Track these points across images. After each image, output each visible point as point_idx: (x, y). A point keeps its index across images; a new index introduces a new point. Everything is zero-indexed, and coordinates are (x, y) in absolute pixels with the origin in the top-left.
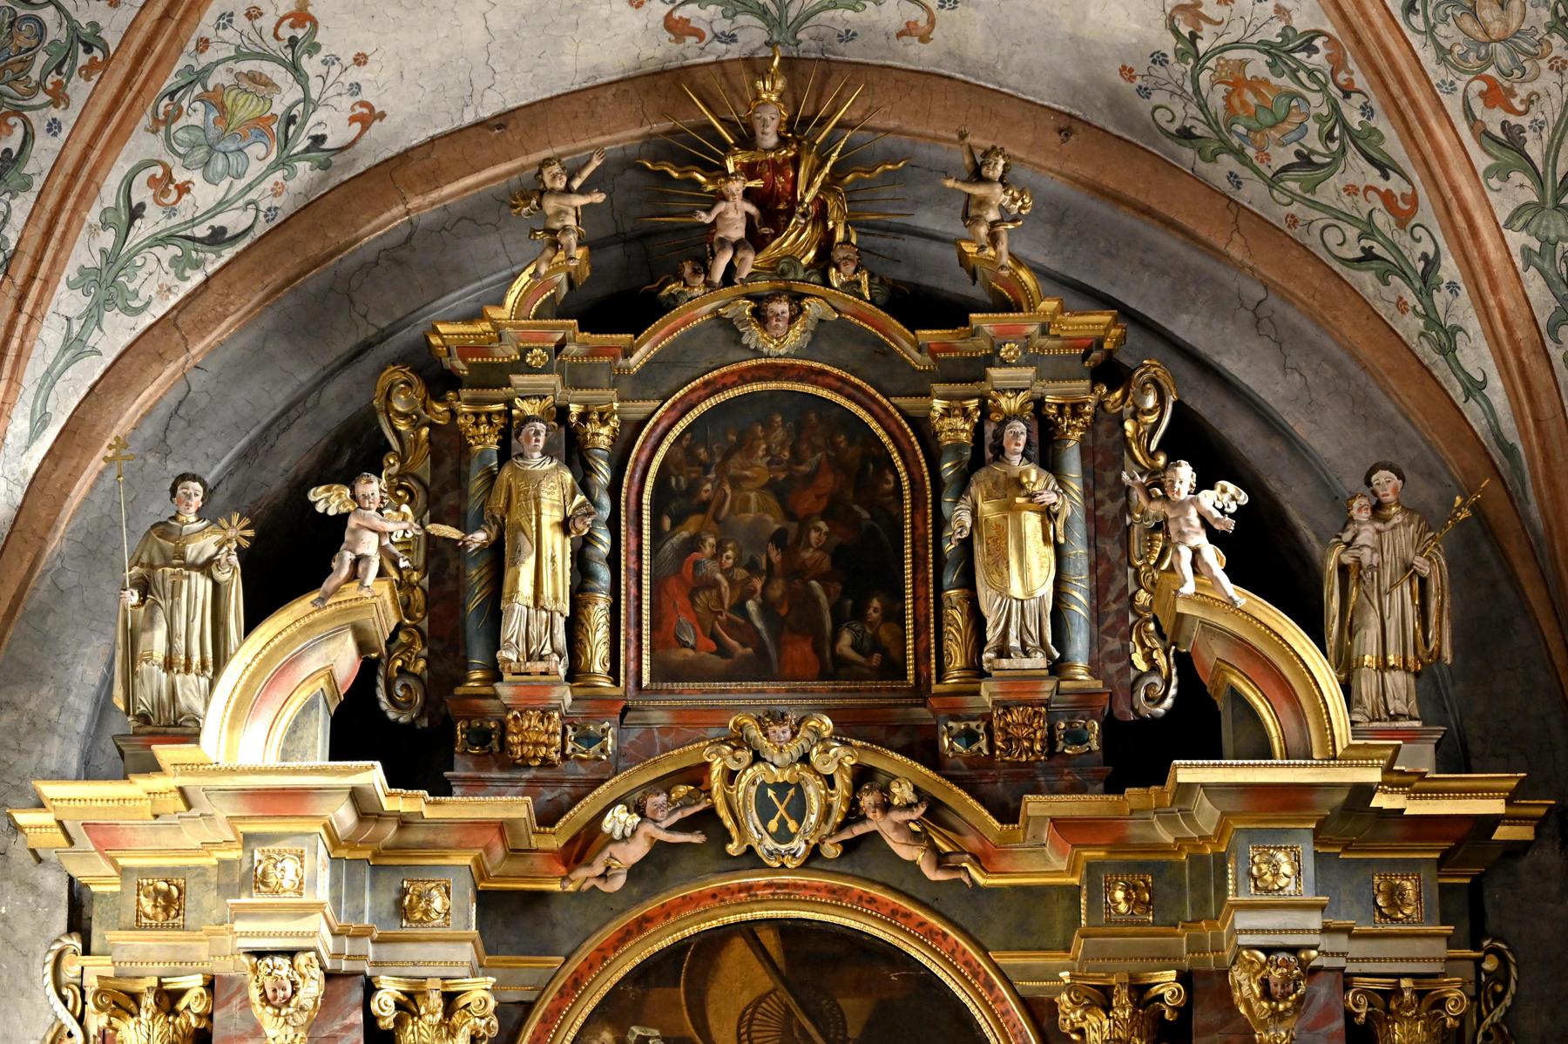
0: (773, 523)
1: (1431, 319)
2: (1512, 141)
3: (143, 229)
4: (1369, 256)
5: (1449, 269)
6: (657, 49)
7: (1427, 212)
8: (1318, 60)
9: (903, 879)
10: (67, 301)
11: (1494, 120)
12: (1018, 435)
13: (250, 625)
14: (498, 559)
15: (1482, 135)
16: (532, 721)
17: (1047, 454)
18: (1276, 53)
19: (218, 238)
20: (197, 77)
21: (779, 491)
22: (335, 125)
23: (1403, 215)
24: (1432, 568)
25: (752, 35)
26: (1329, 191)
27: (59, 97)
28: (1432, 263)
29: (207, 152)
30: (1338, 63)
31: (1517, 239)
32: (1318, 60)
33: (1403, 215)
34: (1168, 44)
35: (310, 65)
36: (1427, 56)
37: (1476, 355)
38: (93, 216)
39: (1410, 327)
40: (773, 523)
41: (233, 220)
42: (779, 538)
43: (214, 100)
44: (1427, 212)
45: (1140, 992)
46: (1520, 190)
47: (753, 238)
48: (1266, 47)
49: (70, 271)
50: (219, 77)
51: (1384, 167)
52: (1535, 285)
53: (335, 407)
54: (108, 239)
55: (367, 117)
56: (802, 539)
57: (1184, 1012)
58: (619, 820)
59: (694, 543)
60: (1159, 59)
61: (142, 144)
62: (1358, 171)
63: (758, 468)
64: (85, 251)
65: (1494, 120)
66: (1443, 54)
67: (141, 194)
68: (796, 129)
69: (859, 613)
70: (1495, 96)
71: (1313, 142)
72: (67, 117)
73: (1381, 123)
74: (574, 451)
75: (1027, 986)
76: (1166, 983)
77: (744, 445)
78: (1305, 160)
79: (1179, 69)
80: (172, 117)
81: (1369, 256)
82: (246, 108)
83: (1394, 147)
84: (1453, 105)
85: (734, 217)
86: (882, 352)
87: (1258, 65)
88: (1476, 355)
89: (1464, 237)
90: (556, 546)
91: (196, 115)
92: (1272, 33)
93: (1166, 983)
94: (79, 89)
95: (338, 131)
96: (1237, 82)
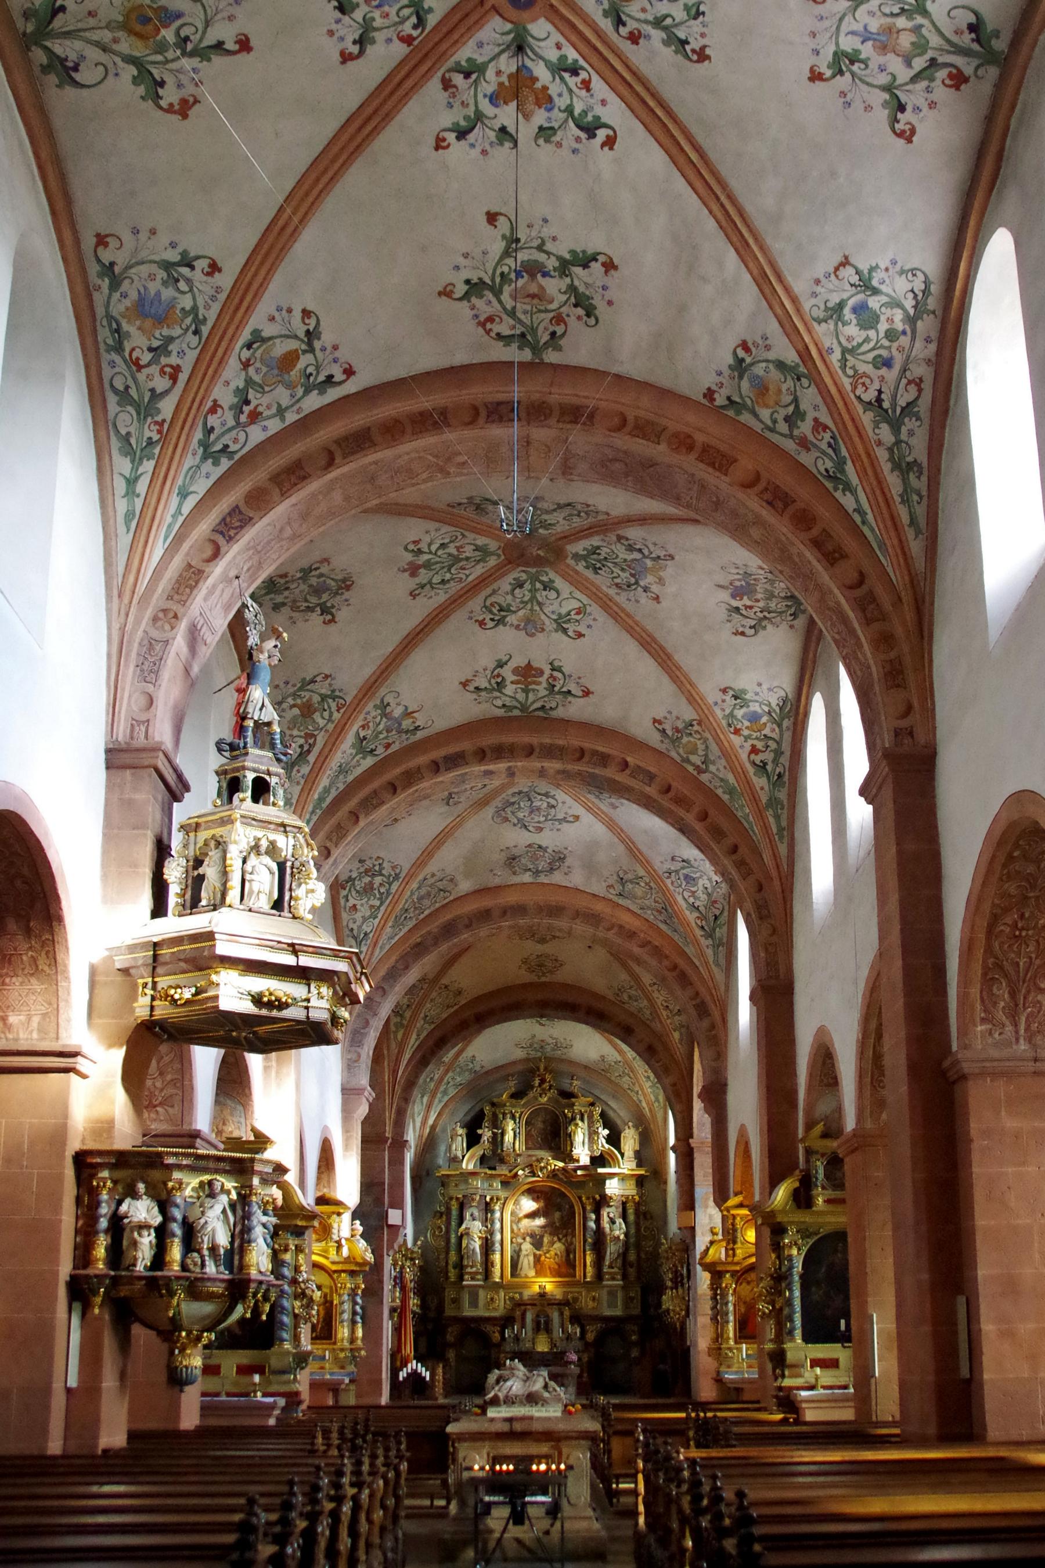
9: (560, 1180)
10: (439, 1095)
13: (468, 1149)
14: (503, 1134)
17: (582, 1120)
22: (478, 1068)
24: (637, 1137)
25: (539, 1054)
29: (460, 1074)
37: (644, 1104)
45: (594, 1199)
46: (649, 1084)
53: (477, 1109)
58: (520, 1172)
61: (450, 1074)
64: (442, 1088)
68: (546, 1069)
74: (513, 1117)
76: (597, 1197)
85: (537, 1082)
89: (642, 1090)
90: (511, 1133)
93: (597, 1197)
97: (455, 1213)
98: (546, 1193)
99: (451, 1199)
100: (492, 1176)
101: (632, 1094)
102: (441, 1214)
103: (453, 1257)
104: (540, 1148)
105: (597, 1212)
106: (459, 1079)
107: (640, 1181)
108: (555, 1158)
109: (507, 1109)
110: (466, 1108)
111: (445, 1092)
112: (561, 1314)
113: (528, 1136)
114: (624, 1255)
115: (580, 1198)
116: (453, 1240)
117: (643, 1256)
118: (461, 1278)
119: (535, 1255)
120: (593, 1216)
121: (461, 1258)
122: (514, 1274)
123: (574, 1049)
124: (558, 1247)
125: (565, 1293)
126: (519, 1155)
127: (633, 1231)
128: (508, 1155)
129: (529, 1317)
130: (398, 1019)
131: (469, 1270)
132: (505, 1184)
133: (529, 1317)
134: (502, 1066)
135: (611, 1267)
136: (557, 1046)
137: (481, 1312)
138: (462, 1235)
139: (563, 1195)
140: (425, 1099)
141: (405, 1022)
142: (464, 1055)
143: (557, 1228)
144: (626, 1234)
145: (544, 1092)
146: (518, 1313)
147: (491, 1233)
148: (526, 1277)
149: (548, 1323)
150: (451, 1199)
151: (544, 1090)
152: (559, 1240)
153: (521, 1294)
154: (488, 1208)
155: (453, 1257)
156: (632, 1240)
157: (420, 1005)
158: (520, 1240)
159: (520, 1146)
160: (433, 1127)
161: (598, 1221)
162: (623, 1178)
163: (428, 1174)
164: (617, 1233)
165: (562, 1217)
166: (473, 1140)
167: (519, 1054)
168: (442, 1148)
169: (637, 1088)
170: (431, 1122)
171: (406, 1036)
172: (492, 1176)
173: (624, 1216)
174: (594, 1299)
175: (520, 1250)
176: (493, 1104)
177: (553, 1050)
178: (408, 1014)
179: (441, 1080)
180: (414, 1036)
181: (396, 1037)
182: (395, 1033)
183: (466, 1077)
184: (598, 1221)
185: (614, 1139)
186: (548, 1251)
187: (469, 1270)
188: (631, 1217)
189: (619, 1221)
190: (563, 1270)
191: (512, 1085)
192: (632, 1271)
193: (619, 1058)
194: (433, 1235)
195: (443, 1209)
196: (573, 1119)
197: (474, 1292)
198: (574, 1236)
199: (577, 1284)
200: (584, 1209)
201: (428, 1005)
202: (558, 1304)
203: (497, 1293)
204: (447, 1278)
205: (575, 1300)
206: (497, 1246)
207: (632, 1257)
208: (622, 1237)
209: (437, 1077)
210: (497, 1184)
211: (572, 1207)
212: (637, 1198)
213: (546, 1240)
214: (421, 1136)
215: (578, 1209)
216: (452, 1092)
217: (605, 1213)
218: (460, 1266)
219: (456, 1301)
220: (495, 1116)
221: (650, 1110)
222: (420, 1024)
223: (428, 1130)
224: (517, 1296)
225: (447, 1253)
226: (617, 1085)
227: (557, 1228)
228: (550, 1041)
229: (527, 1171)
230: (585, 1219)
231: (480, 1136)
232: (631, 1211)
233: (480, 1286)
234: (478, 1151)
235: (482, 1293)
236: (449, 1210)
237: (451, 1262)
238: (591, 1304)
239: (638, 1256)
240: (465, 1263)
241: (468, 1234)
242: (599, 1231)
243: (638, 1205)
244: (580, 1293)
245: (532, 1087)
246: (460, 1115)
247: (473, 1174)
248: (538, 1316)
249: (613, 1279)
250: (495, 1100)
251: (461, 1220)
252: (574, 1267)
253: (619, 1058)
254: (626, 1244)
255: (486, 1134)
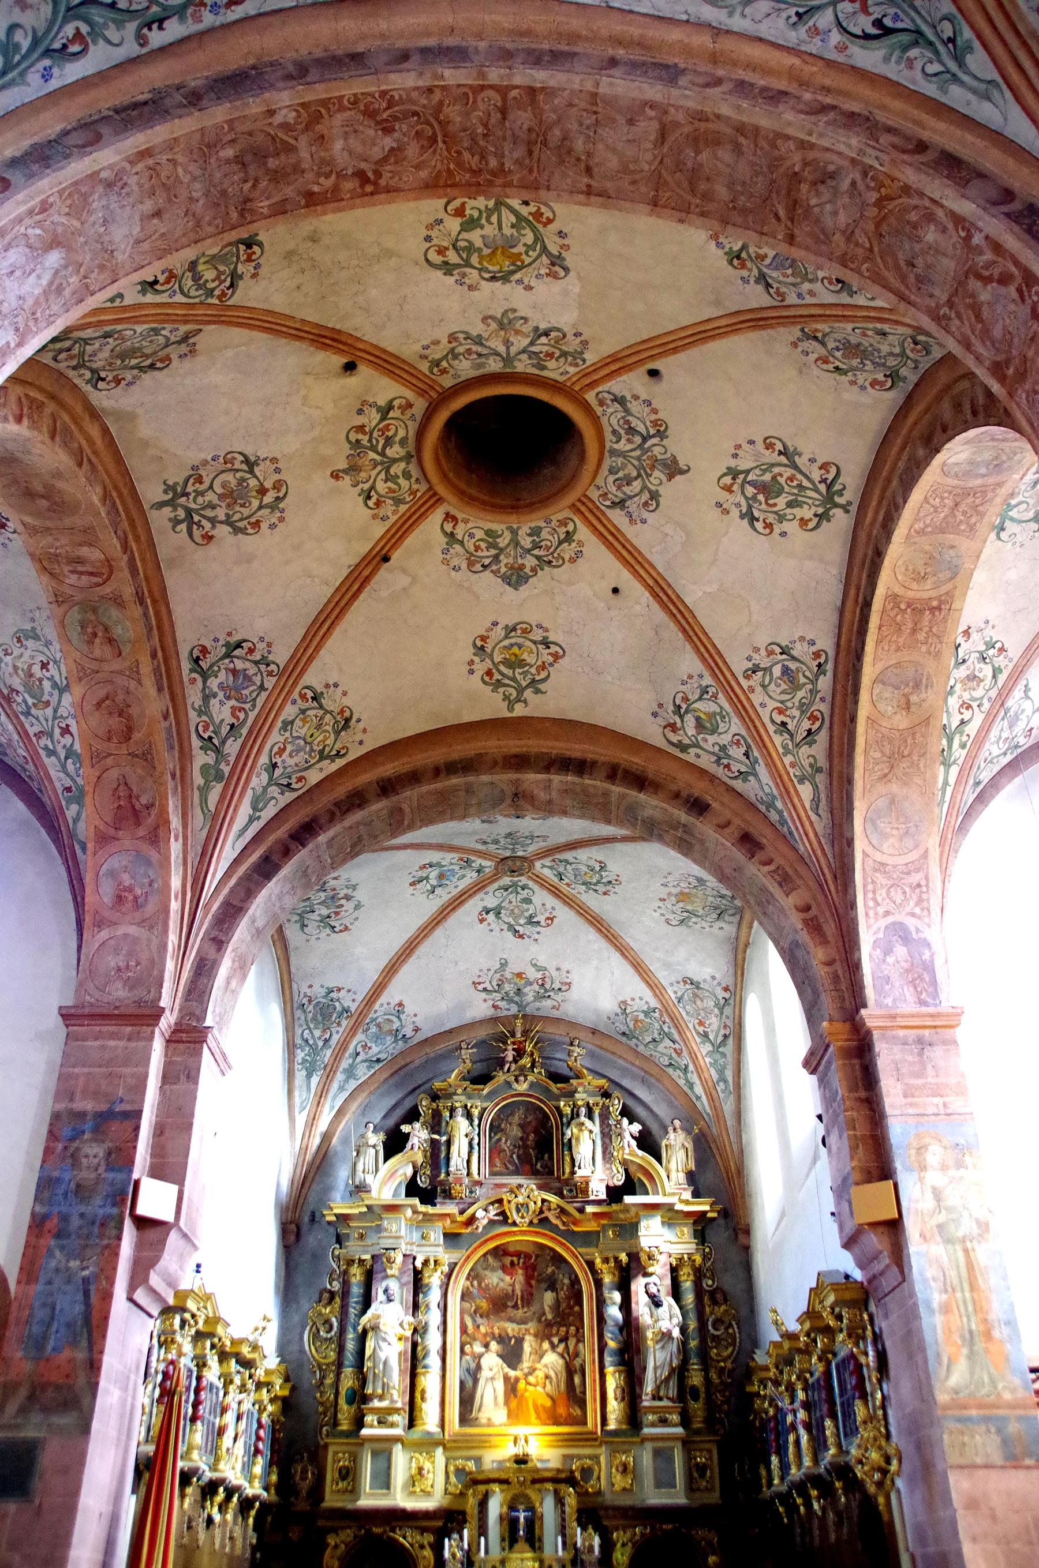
0: (520, 1134)
1: (687, 1081)
2: (705, 1035)
3: (359, 1059)
4: (671, 1064)
5: (691, 1067)
6: (490, 1012)
7: (685, 1053)
8: (657, 1015)
9: (554, 1228)
10: (340, 1077)
11: (701, 1029)
12: (583, 1110)
13: (386, 1160)
14: (449, 1143)
15: (698, 1033)
16: (458, 1187)
17: (590, 1116)
18: (646, 1013)
19: (378, 1060)
20: (373, 1020)
21: (522, 1126)
23: (679, 1053)
24: (690, 1146)
25: (514, 1009)
26: (661, 1048)
27: (339, 1024)
28: (686, 1066)
29: (377, 1038)
30: (661, 1015)
31: (708, 1060)
32: (657, 1015)
33: (679, 1053)
34: (619, 1011)
35: (403, 1017)
36: (684, 1014)
37: (699, 1090)
38: (347, 1055)
39: (682, 1082)
40: (520, 1134)
41: (382, 1056)
42: (521, 1139)
43: (378, 1026)
44: (685, 1053)
45: (616, 1259)
46: (708, 1047)
47: (515, 1061)
48: (643, 1012)
49: (341, 1069)
50: (379, 1020)
51: (674, 1042)
52: (713, 1072)
53: (408, 1104)
54: (350, 1061)
55: (417, 1030)
56: (527, 1139)
57: (628, 1264)
58: (480, 1214)
59: (499, 1140)
60: (617, 1015)
61: (360, 1037)
62: (667, 1042)
63: (516, 1119)
64: (345, 1064)
65: (701, 1029)
66: (688, 1013)
67: (359, 1049)
68: (525, 1033)
69: (542, 1158)
70: (701, 1023)
71: (656, 1035)
72: (341, 1030)
73: (673, 1031)
74: (469, 1116)
75: (588, 1257)
76: (623, 1257)
77: (512, 1114)
78: (654, 1040)
79: (622, 1017)
80: (368, 1030)
81: (671, 1064)
82: (386, 1027)
83: (676, 1036)
84: (691, 1026)
85: (510, 1055)
86: (547, 1091)
87: (641, 1016)
88: (699, 1090)
90: (465, 1142)
91: (374, 1029)
92: (645, 1008)
93: (623, 1257)
94: (344, 1023)
95: (409, 1032)
96: (636, 1021)
97: (356, 1290)
98: (528, 1256)
99: (350, 1262)
100: (428, 1218)
101: (676, 1074)
102: (332, 1295)
103: (348, 1381)
104: (517, 1172)
105: (624, 1287)
106: (375, 1049)
107: (701, 1225)
108: (540, 1187)
109: (459, 1100)
110: (389, 1102)
111: (350, 1073)
112: (560, 1501)
113: (495, 1150)
114: (680, 1372)
115: (591, 1264)
116: (350, 1345)
117: (714, 1376)
118: (359, 1423)
119: (506, 1378)
120: (617, 1296)
121: (363, 1382)
122: (465, 1419)
123: (574, 994)
124: (552, 1360)
125: (566, 1458)
126: (480, 1183)
127: (692, 1325)
128: (459, 1181)
129: (495, 1507)
130: (210, 758)
131: (376, 1403)
132: (451, 1238)
133: (495, 1507)
134: (450, 1031)
135: (656, 1397)
136: (545, 991)
137: (401, 1500)
138: (365, 1332)
139: (558, 1260)
140: (315, 1080)
141: (226, 770)
142: (383, 999)
143: (549, 1325)
144: (683, 1330)
145: (522, 1072)
146: (471, 1504)
147: (419, 1329)
148: (490, 1424)
149: (531, 1524)
150: (350, 1262)
151: (522, 1069)
152: (553, 1347)
153: (478, 1460)
154: (418, 1285)
155: (348, 1381)
156: (693, 1344)
157: (258, 732)
158: (478, 1348)
159: (480, 1169)
160: (326, 1137)
161: (626, 1306)
162: (671, 1216)
163: (313, 1218)
164: (665, 1325)
165: (558, 1302)
166: (395, 1143)
167: (480, 1008)
168: (342, 1175)
169: (685, 1060)
170: (323, 1124)
171: (227, 801)
172: (428, 1218)
173: (676, 1293)
174: (625, 1469)
175: (479, 1367)
176: (435, 1097)
177: (539, 997)
178: (232, 748)
179: (343, 1046)
180: (245, 810)
181: (204, 801)
182: (204, 790)
183: (385, 1048)
184: (626, 1306)
185: (648, 1142)
186: (532, 1371)
187: (376, 1403)
188: (689, 1298)
189: (668, 1301)
190: (562, 1410)
191: (466, 1061)
192: (697, 1407)
193: (654, 1003)
194: (316, 1336)
195: (336, 1286)
196: (575, 1115)
197: (383, 1449)
198: (580, 1339)
199: (588, 1439)
200: (599, 1284)
201: (276, 737)
202: (554, 1480)
203: (431, 1457)
204: (336, 1423)
205: (587, 1472)
206: (433, 1361)
207: (696, 1379)
208: (676, 1333)
209: (335, 1038)
210: (436, 1235)
211: (575, 1281)
212: (698, 1259)
213: (527, 1347)
214: (304, 1149)
215: (587, 1287)
216: (363, 1073)
217: (638, 1286)
218: (360, 1398)
219: (349, 1474)
220: (437, 1115)
221: (711, 1098)
222: (259, 780)
223: (316, 1141)
224: (471, 1465)
225: (338, 1375)
226: (648, 1059)
227: (549, 1325)
228: (532, 974)
229: (493, 1211)
230: (601, 1303)
231: (407, 1137)
232: (687, 1284)
233: (397, 1439)
234: (401, 1167)
235: (400, 1459)
236: (346, 1285)
237: (343, 1392)
238: (620, 1481)
239: (707, 1380)
240: (369, 1391)
241: (375, 1328)
242: (630, 1326)
243: (699, 1274)
244: (596, 1458)
245: (501, 1063)
246: (377, 1117)
247: (392, 1208)
248: (512, 1508)
249: (664, 1422)
250: (437, 1085)
251: (367, 1302)
252: (582, 1403)
253: (654, 1003)
254: (684, 1344)
255: (418, 1134)
